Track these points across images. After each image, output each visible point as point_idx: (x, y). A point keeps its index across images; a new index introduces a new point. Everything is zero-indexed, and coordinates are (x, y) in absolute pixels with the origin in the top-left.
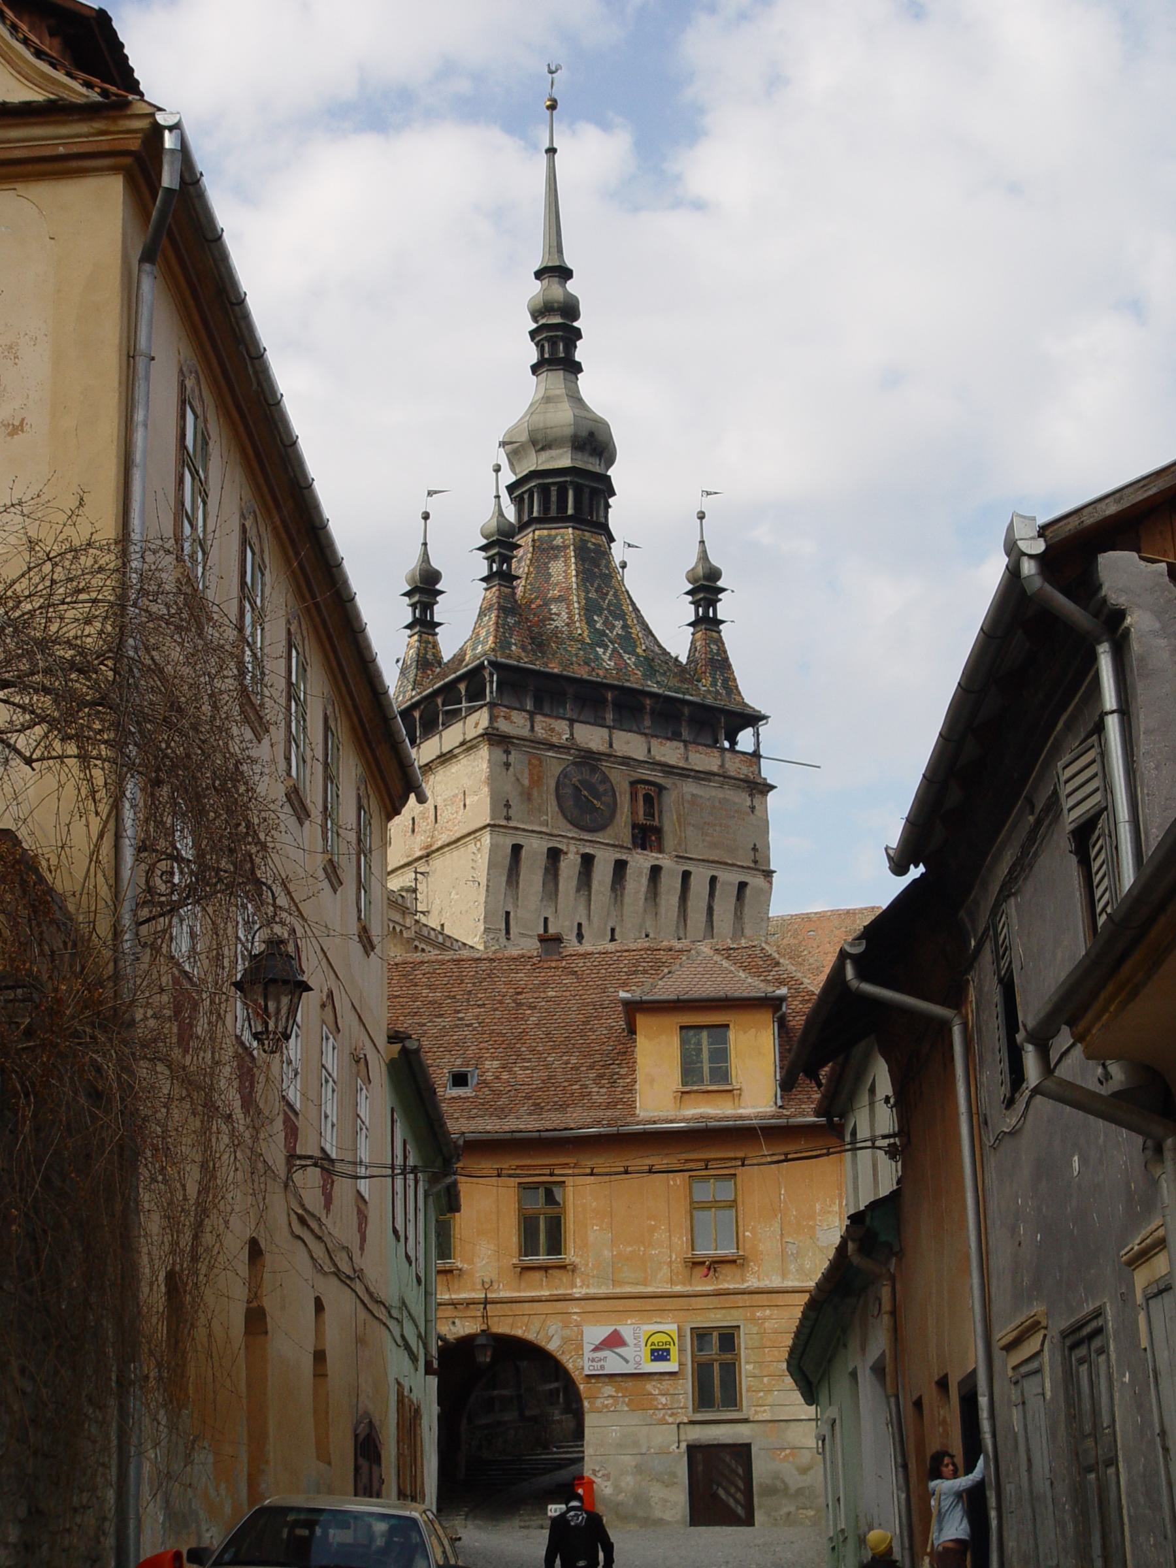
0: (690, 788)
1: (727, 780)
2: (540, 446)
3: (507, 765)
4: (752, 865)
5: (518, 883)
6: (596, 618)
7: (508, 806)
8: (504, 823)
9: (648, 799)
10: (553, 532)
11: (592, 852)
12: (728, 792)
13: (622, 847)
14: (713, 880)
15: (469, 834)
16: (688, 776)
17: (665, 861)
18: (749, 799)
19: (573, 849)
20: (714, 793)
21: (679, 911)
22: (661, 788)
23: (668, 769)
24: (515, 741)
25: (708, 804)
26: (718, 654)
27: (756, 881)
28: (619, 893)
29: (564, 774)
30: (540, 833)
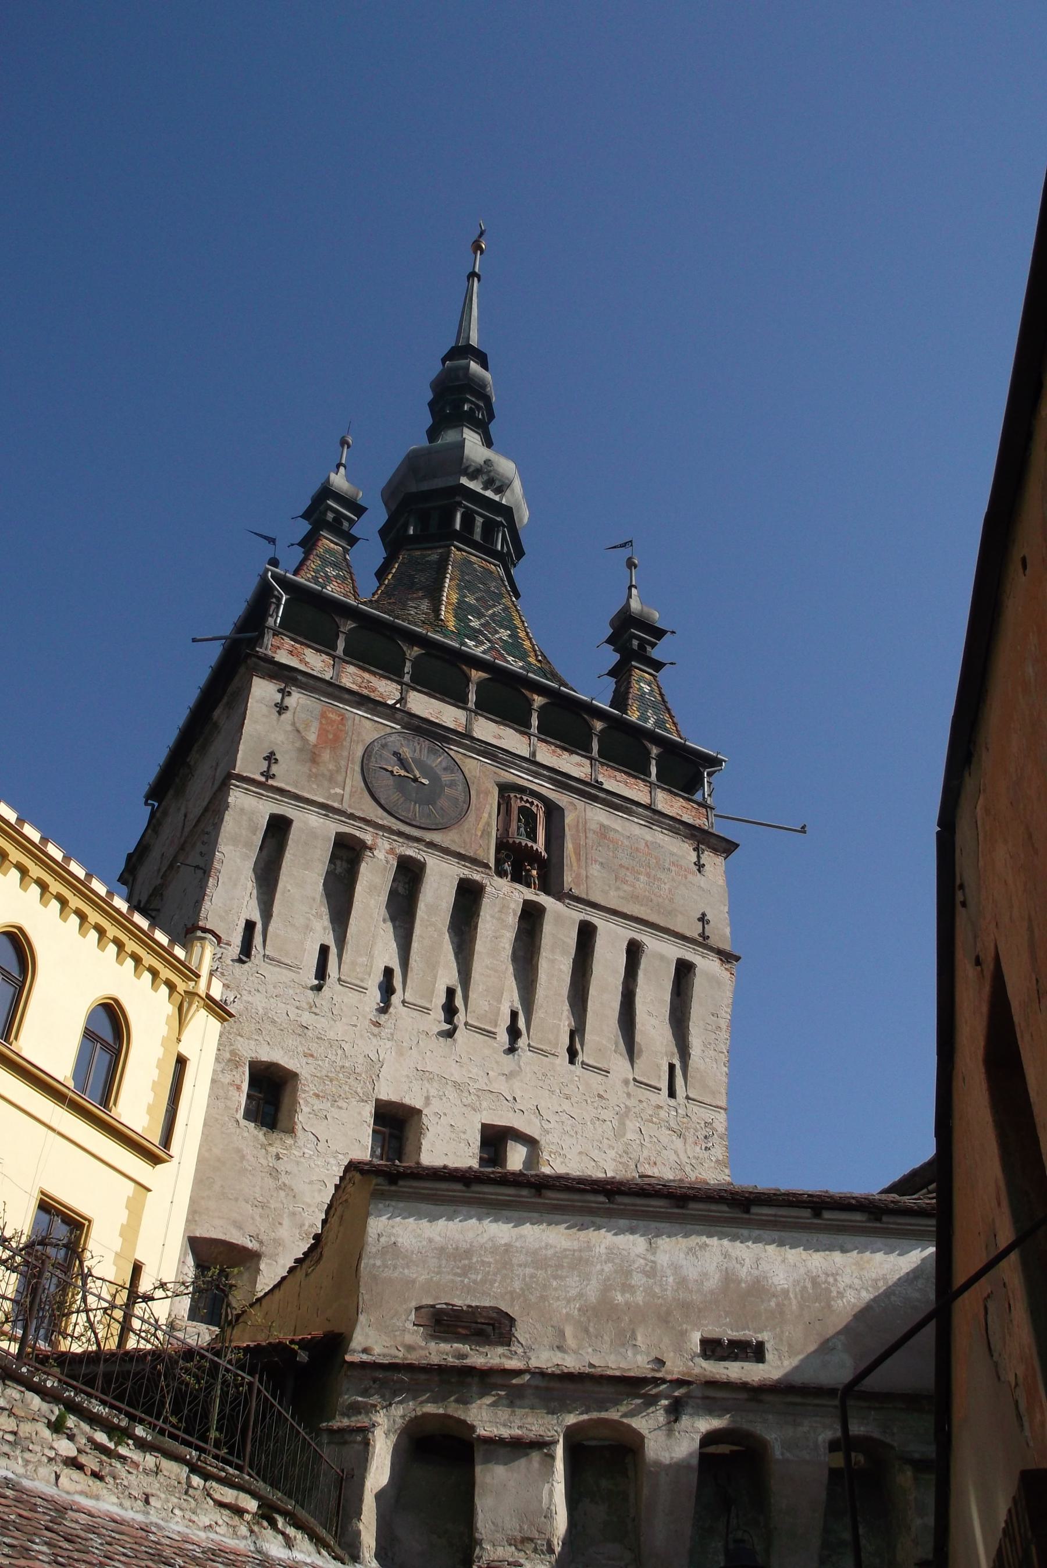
0: (598, 815)
3: (281, 708)
4: (700, 939)
6: (470, 617)
7: (271, 758)
8: (263, 779)
9: (528, 817)
11: (419, 857)
12: (661, 836)
13: (475, 862)
14: (634, 951)
15: (206, 809)
16: (595, 799)
18: (694, 854)
23: (562, 780)
25: (626, 842)
26: (650, 694)
27: (706, 965)
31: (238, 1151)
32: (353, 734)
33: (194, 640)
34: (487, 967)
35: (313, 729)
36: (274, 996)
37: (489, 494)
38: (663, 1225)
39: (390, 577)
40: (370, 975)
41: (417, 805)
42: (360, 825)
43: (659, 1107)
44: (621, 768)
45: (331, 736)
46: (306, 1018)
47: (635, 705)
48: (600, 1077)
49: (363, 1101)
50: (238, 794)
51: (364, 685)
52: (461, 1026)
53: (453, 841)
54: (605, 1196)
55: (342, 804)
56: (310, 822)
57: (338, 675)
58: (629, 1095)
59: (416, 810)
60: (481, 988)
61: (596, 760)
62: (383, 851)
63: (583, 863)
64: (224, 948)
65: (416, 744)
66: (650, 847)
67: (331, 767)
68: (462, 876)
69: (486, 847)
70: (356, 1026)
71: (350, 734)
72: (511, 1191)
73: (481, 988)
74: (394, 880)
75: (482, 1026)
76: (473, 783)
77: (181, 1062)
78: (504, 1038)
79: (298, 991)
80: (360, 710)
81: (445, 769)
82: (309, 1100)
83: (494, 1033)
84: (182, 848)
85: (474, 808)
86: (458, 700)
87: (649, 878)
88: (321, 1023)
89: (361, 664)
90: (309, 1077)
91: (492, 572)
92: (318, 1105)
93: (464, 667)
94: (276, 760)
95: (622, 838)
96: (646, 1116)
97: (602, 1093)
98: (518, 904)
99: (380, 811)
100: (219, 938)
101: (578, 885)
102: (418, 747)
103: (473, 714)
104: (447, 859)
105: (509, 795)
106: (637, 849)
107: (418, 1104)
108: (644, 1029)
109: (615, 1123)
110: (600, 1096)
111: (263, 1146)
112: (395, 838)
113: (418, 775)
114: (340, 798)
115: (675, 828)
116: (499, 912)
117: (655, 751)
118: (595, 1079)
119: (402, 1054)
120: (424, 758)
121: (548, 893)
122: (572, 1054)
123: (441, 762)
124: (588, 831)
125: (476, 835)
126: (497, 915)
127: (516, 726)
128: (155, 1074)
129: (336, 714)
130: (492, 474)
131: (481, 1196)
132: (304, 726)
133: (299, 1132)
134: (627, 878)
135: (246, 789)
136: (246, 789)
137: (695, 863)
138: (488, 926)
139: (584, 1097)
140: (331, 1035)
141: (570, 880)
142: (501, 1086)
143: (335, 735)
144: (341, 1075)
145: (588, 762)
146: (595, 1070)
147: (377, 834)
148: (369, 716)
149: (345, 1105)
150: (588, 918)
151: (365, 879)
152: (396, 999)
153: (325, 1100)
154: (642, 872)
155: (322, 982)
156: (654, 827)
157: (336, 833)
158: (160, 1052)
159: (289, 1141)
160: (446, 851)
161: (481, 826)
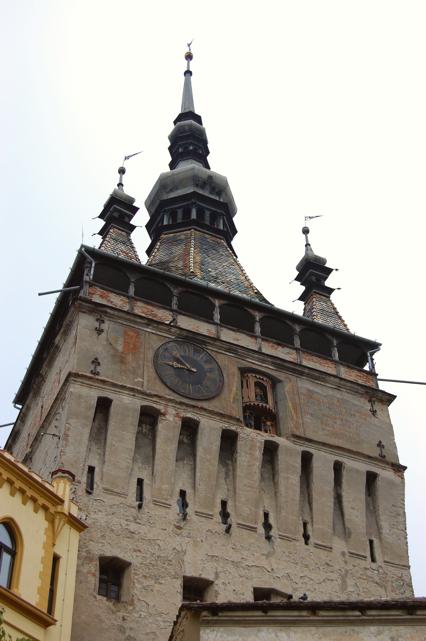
1: (342, 382)
2: (169, 190)
3: (99, 331)
5: (105, 439)
7: (96, 362)
10: (178, 234)
11: (195, 418)
12: (347, 395)
15: (57, 399)
16: (301, 373)
17: (281, 441)
19: (171, 411)
20: (331, 392)
21: (302, 492)
22: (275, 382)
24: (109, 311)
28: (231, 468)
29: (164, 348)
30: (132, 390)
31: (98, 616)
32: (145, 344)
33: (40, 294)
34: (246, 485)
35: (120, 342)
36: (111, 513)
37: (211, 196)
38: (401, 628)
39: (156, 250)
40: (171, 496)
41: (191, 385)
42: (155, 400)
43: (366, 569)
44: (316, 353)
45: (131, 346)
46: (133, 527)
47: (318, 315)
48: (326, 552)
49: (175, 578)
50: (75, 386)
51: (149, 313)
52: (234, 526)
53: (216, 406)
54: (359, 611)
55: (143, 388)
56: (124, 401)
57: (132, 308)
58: (346, 562)
59: (190, 389)
60: (243, 499)
61: (299, 350)
62: (172, 416)
63: (299, 415)
64: (77, 485)
65: (186, 347)
66: (340, 402)
67: (133, 365)
68: (224, 428)
69: (237, 409)
70: (165, 530)
71: (144, 344)
72: (296, 613)
73: (243, 499)
74: (181, 434)
75: (246, 524)
76: (224, 369)
77: (56, 559)
78: (261, 530)
79: (126, 510)
80: (149, 328)
81: (206, 362)
82: (140, 580)
83: (256, 528)
84: (42, 427)
85: (226, 385)
86: (209, 319)
87: (342, 421)
88: (144, 529)
89: (146, 300)
90: (138, 565)
91: (219, 243)
92: (146, 583)
93: (210, 298)
94: (99, 363)
95: (322, 398)
96: (358, 575)
97: (329, 562)
98: (261, 444)
99: (168, 391)
100: (73, 476)
101: (297, 428)
102: (187, 349)
103: (219, 327)
104: (213, 418)
105: (248, 376)
106: (333, 404)
107: (211, 578)
108: (350, 518)
109: (340, 581)
110: (327, 564)
111: (113, 612)
112: (179, 407)
113: (189, 367)
114: (141, 384)
115: (355, 388)
116: (250, 449)
117: (335, 342)
118: (322, 554)
119: (197, 546)
120: (191, 355)
121: (280, 435)
122: (306, 537)
123: (202, 357)
124: (300, 394)
125: (230, 401)
126: (248, 452)
127: (247, 332)
128: (40, 567)
129: (133, 331)
130: (213, 185)
131: (275, 618)
132: (114, 341)
133: (136, 602)
134: (328, 422)
135: (82, 383)
136: (82, 383)
137: (370, 410)
138: (243, 459)
139: (317, 566)
140: (150, 536)
141: (293, 425)
142: (264, 562)
143: (134, 345)
144: (159, 562)
145: (295, 351)
146: (323, 548)
147: (167, 405)
148: (154, 332)
149: (163, 581)
150: (307, 449)
151: (163, 434)
152: (188, 510)
153: (150, 579)
154: (337, 418)
155: (141, 502)
156: (342, 389)
157: (141, 406)
158: (42, 553)
159: (130, 608)
160: (212, 412)
161: (232, 396)
